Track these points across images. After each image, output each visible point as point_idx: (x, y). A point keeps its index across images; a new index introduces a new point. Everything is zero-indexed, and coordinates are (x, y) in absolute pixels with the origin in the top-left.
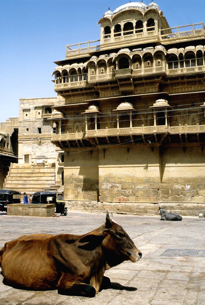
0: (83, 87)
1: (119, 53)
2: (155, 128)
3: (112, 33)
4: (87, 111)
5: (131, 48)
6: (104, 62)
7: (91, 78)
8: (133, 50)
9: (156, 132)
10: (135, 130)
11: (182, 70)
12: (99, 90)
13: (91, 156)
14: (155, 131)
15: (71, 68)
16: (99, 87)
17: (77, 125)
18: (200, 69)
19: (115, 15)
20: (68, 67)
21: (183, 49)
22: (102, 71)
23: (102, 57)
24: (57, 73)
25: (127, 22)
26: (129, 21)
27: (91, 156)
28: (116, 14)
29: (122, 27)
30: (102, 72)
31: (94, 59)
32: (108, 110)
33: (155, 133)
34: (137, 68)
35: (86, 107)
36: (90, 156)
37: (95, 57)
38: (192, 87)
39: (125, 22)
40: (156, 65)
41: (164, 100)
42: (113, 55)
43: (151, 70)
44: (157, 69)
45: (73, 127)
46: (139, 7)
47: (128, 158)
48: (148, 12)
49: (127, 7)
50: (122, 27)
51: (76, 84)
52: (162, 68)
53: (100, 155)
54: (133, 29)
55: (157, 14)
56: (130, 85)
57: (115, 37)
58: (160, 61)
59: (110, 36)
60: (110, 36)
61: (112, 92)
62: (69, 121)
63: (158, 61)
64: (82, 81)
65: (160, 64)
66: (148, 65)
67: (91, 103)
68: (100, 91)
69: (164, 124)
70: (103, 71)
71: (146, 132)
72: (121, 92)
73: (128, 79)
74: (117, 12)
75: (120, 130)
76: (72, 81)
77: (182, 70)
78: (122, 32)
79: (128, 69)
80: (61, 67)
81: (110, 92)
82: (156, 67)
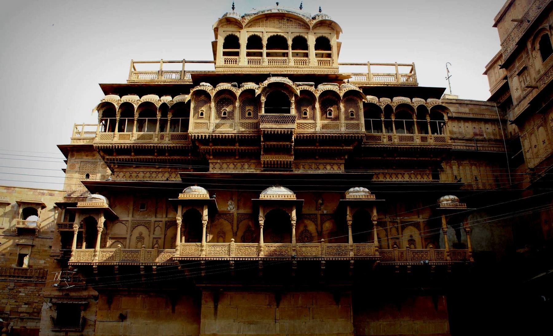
0: (169, 145)
1: (266, 83)
2: (352, 248)
3: (243, 50)
4: (181, 196)
5: (294, 78)
6: (227, 96)
7: (197, 124)
8: (296, 83)
9: (353, 256)
10: (304, 249)
11: (390, 138)
12: (210, 155)
13: (173, 311)
14: (352, 254)
15: (143, 102)
16: (211, 147)
17: (141, 234)
18: (424, 139)
19: (249, 19)
20: (134, 99)
21: (390, 100)
22: (225, 114)
23: (224, 86)
24: (104, 109)
25: (275, 34)
26: (279, 34)
27: (173, 311)
28: (252, 17)
29: (265, 42)
30: (222, 116)
31: (206, 86)
32: (229, 202)
33: (352, 258)
34: (305, 118)
35: (181, 187)
36: (169, 310)
37: (208, 84)
38: (404, 174)
39: (272, 34)
40: (347, 118)
41: (367, 190)
42: (250, 85)
43: (337, 126)
44: (347, 126)
45: (128, 236)
46: (299, 14)
47: (278, 315)
48: (319, 25)
49: (275, 9)
50: (265, 42)
51: (151, 139)
52: (358, 124)
53: (203, 309)
54: (287, 48)
55: (335, 31)
56: (286, 151)
57: (249, 58)
58: (354, 111)
59: (237, 54)
60: (237, 54)
61: (239, 164)
62: (121, 222)
63: (350, 111)
64: (166, 134)
65: (354, 117)
66: (328, 116)
67: (189, 182)
68: (211, 157)
69: (371, 240)
70: (227, 116)
71: (330, 254)
72: (263, 166)
73: (287, 136)
74: (255, 14)
75: (267, 249)
76: (140, 129)
77: (390, 138)
78: (265, 51)
79: (288, 115)
80: (117, 97)
81: (235, 164)
82: (346, 122)
